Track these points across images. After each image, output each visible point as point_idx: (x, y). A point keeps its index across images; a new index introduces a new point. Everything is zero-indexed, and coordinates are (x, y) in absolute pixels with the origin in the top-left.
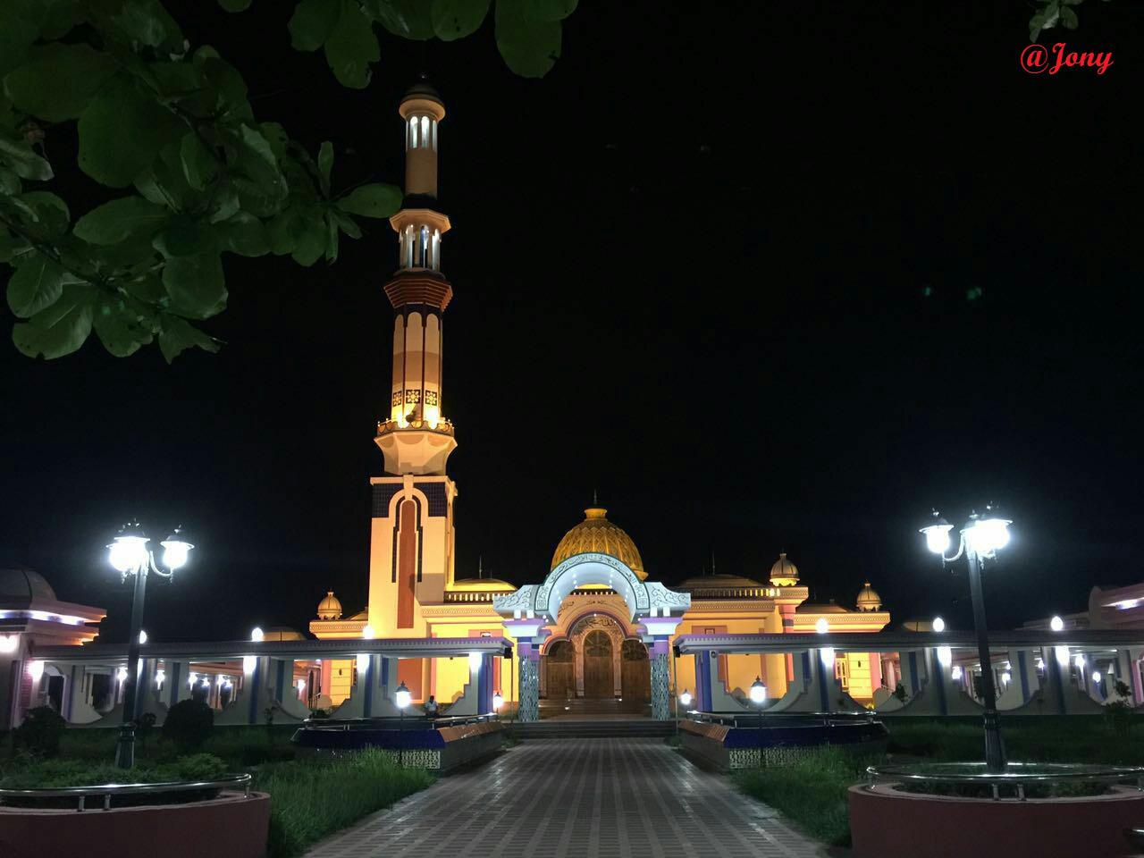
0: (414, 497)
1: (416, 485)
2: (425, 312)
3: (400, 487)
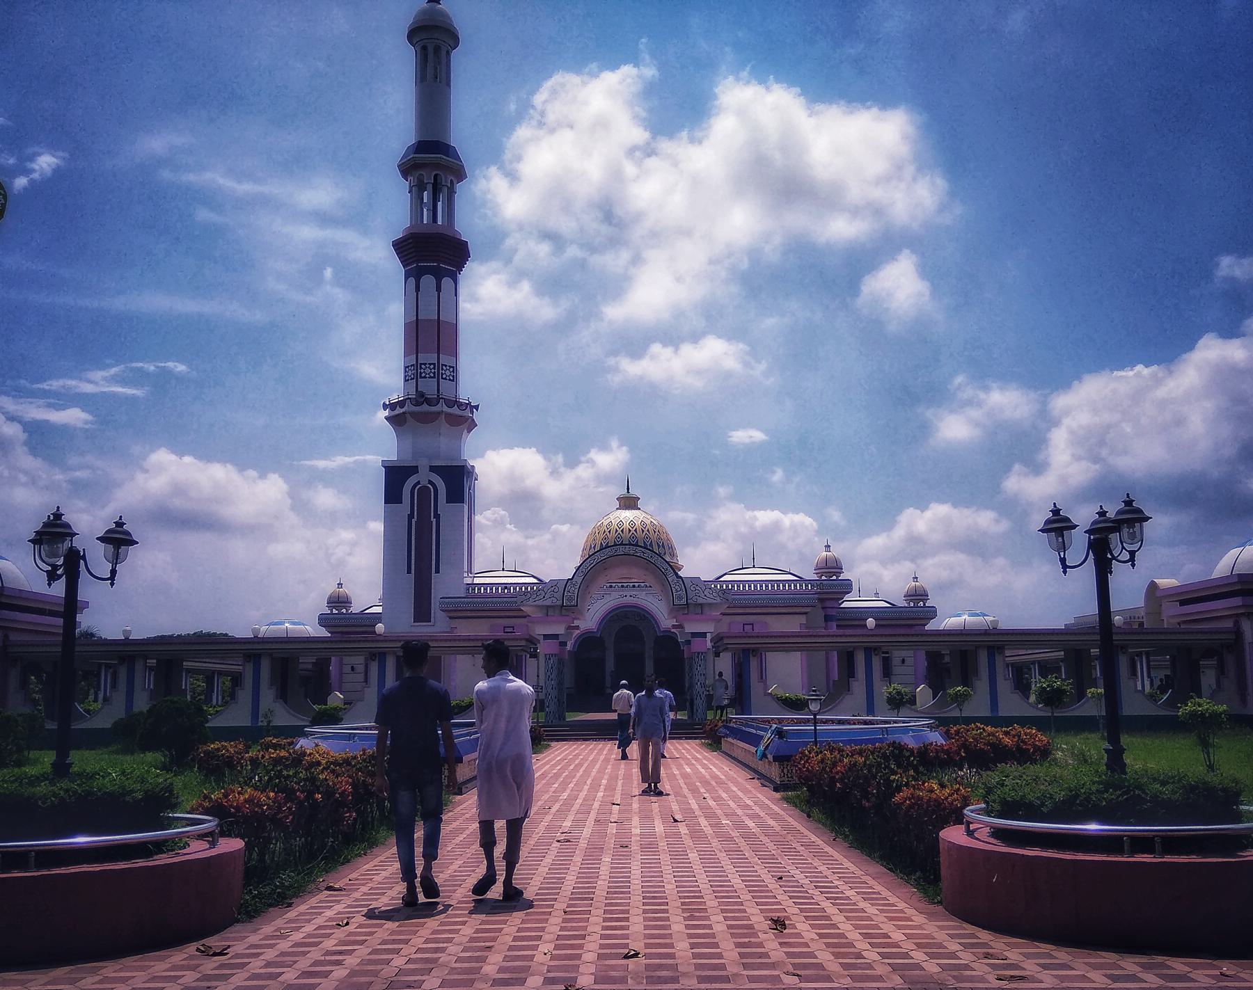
0: (430, 482)
1: (433, 469)
3: (414, 470)
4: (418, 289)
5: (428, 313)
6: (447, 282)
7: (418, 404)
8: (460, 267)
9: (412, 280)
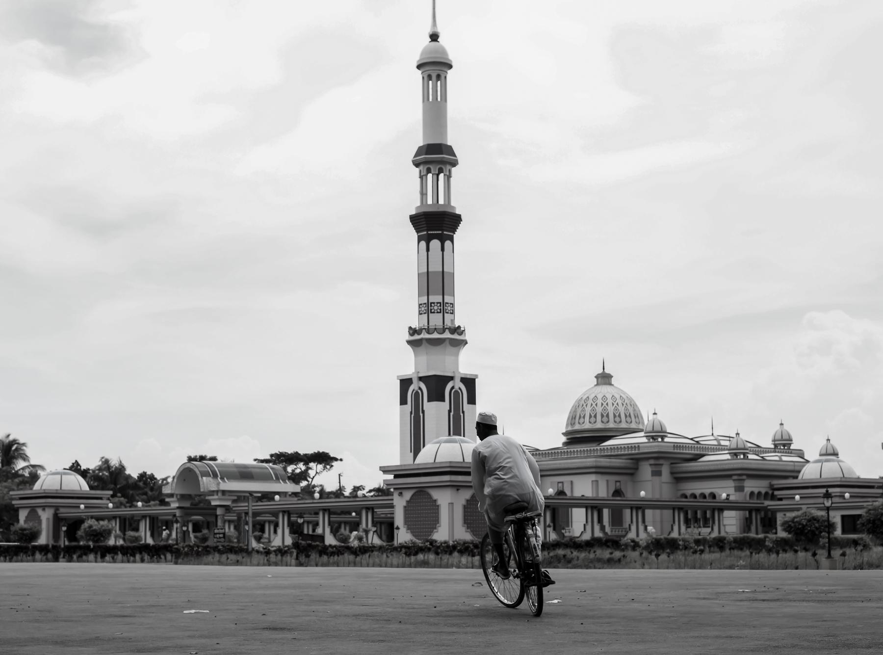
2: (442, 239)
4: (428, 250)
5: (435, 267)
6: (448, 243)
7: (428, 331)
8: (454, 231)
9: (423, 244)
